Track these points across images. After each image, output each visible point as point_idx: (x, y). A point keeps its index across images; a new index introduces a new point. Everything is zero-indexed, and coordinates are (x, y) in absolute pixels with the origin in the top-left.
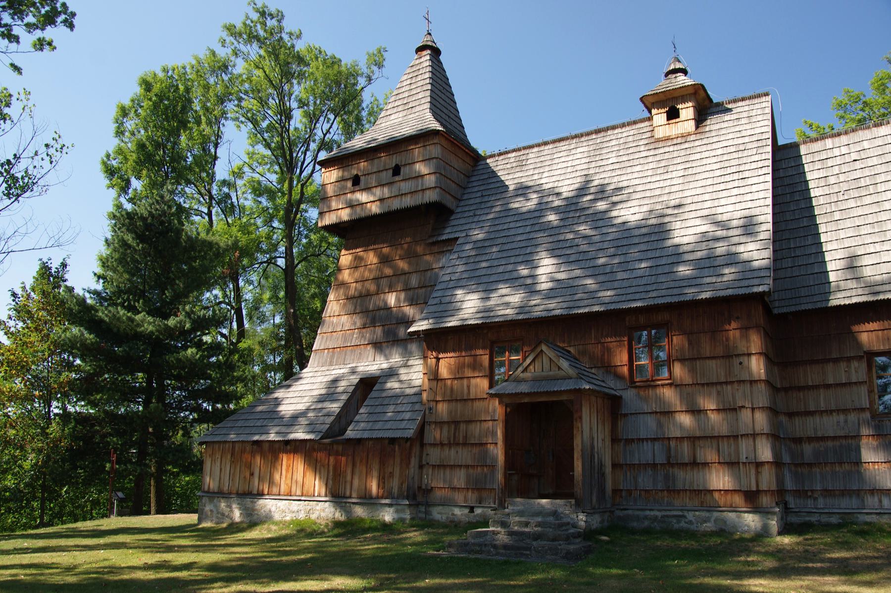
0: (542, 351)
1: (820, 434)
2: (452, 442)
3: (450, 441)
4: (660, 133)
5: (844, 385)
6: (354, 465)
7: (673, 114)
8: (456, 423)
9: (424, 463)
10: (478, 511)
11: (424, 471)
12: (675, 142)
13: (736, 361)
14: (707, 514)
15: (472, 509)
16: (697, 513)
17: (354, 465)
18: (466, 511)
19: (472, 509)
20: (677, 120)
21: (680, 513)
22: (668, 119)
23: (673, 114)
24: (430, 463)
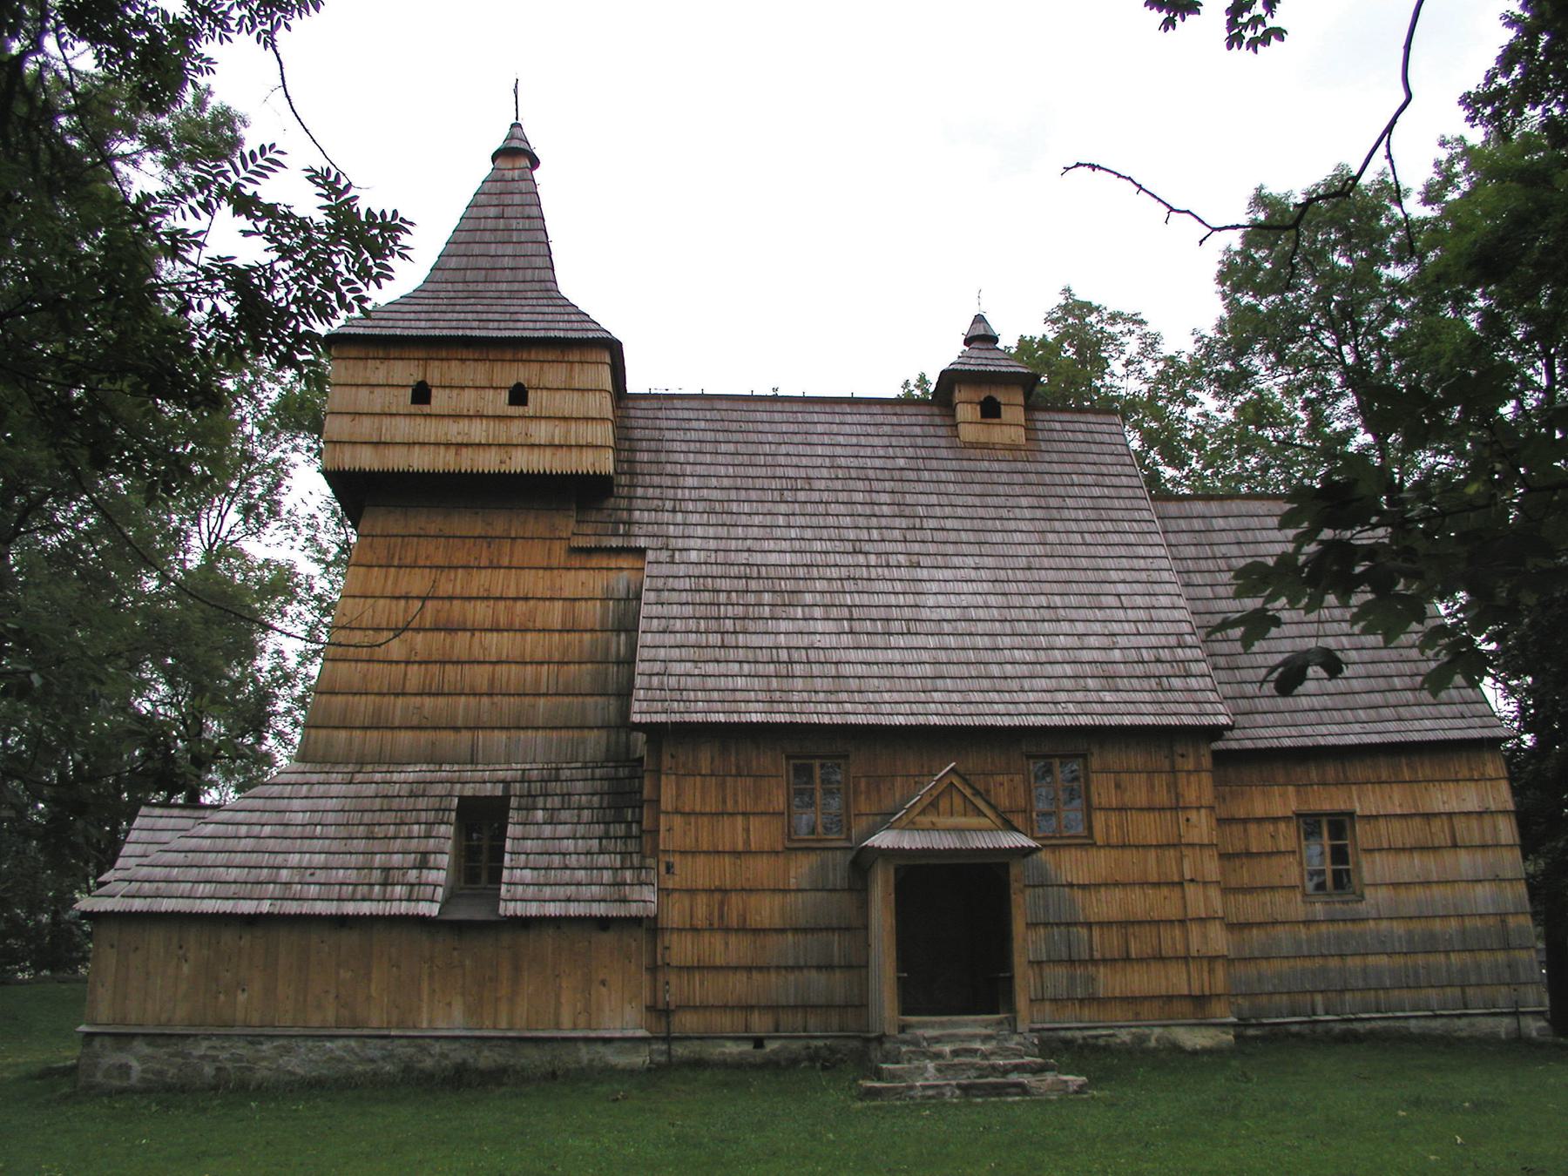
0: (952, 783)
1: (1242, 920)
2: (716, 926)
3: (711, 924)
4: (968, 433)
5: (1269, 854)
6: (517, 969)
7: (990, 410)
8: (724, 891)
9: (659, 962)
10: (771, 1046)
11: (661, 978)
12: (1000, 455)
13: (1182, 816)
14: (1147, 1031)
15: (759, 1043)
16: (1134, 1030)
17: (517, 969)
18: (747, 1047)
19: (759, 1043)
20: (996, 421)
21: (1111, 1032)
22: (983, 416)
23: (990, 410)
24: (674, 963)
